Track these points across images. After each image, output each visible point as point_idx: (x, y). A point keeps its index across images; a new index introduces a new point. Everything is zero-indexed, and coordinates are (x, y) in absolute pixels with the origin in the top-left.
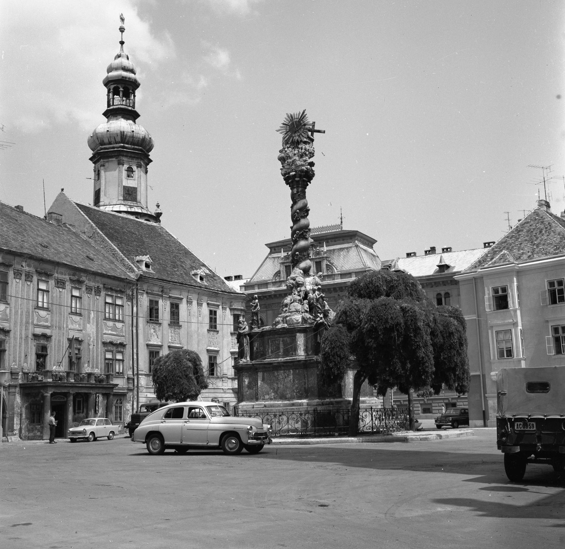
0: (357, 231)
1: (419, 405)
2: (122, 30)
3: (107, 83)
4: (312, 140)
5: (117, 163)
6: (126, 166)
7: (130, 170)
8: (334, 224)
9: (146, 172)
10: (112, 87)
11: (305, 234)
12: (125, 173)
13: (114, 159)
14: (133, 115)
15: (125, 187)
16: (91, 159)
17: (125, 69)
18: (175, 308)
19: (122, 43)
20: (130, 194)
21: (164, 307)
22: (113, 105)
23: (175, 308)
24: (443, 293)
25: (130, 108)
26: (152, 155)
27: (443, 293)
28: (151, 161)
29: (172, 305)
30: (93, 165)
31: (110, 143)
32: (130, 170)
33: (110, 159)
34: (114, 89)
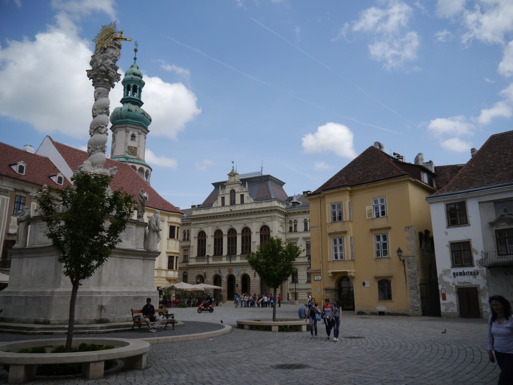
0: (269, 176)
1: (306, 293)
2: (136, 51)
4: (120, 47)
5: (125, 131)
6: (131, 133)
7: (133, 137)
9: (145, 138)
11: (100, 128)
12: (130, 138)
13: (123, 129)
15: (129, 147)
17: (134, 74)
19: (135, 59)
20: (133, 151)
28: (149, 131)
31: (122, 118)
32: (133, 137)
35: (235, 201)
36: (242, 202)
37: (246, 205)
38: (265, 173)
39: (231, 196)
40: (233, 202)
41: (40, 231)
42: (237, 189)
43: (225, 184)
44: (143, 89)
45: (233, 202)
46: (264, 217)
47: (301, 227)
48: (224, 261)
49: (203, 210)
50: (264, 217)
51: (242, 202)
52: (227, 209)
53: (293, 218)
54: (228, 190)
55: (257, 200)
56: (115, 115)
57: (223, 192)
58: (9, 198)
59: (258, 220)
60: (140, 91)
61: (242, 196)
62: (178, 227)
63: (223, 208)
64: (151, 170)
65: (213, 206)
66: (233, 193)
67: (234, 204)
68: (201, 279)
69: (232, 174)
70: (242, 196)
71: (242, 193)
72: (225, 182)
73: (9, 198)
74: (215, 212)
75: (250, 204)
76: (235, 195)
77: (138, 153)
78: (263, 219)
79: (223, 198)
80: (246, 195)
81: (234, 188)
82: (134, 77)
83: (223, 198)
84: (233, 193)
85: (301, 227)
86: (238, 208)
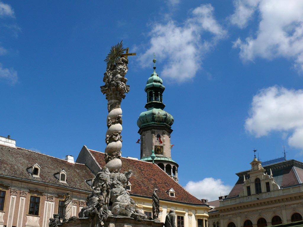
0: (293, 160)
3: (147, 89)
8: (280, 157)
10: (149, 91)
11: (114, 137)
13: (149, 131)
16: (139, 132)
26: (172, 127)
30: (140, 136)
33: (148, 131)
35: (260, 189)
36: (268, 190)
37: (272, 193)
38: (288, 158)
40: (258, 190)
43: (248, 173)
44: (163, 94)
45: (258, 190)
46: (294, 204)
49: (229, 201)
50: (294, 204)
51: (268, 190)
52: (253, 199)
58: (54, 203)
60: (161, 95)
62: (206, 221)
63: (249, 197)
64: (178, 166)
66: (258, 182)
67: (261, 192)
69: (255, 164)
70: (268, 184)
71: (267, 181)
72: (249, 171)
73: (54, 203)
76: (260, 184)
77: (164, 151)
78: (293, 206)
79: (249, 188)
81: (258, 177)
83: (249, 188)
84: (258, 182)
86: (265, 196)
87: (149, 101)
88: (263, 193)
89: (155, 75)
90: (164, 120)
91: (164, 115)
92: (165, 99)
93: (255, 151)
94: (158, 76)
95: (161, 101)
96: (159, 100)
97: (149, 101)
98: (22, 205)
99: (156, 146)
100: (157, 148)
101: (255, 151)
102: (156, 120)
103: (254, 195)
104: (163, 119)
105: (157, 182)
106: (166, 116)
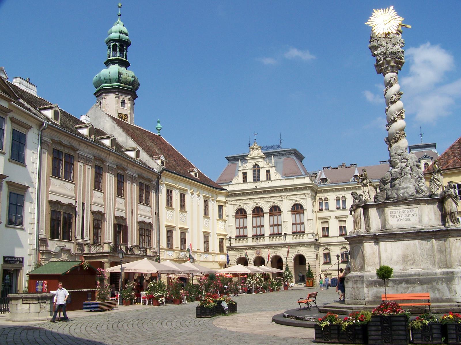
10: (112, 44)
14: (125, 64)
16: (95, 94)
17: (121, 32)
18: (182, 197)
21: (176, 195)
22: (112, 56)
23: (182, 197)
24: (340, 197)
25: (124, 59)
26: (138, 92)
27: (340, 197)
29: (181, 194)
31: (111, 82)
34: (113, 45)
35: (259, 177)
36: (268, 178)
39: (254, 171)
40: (257, 178)
41: (391, 217)
42: (262, 163)
45: (257, 178)
47: (333, 204)
48: (250, 242)
51: (268, 178)
52: (250, 186)
53: (323, 196)
54: (250, 165)
55: (286, 176)
56: (102, 78)
57: (244, 167)
59: (288, 198)
61: (268, 172)
63: (246, 184)
65: (233, 182)
66: (256, 169)
67: (259, 180)
68: (260, 261)
70: (268, 172)
71: (268, 169)
74: (235, 189)
75: (277, 180)
76: (259, 171)
79: (245, 174)
80: (273, 171)
81: (257, 163)
82: (122, 35)
83: (245, 174)
84: (256, 169)
85: (333, 204)
86: (263, 184)
87: (111, 56)
88: (262, 181)
89: (120, 24)
90: (131, 83)
91: (132, 77)
92: (131, 55)
93: (255, 135)
94: (123, 26)
95: (126, 58)
96: (125, 57)
97: (111, 56)
98: (88, 176)
99: (120, 114)
100: (121, 116)
101: (255, 135)
102: (121, 81)
103: (251, 182)
104: (130, 81)
105: (175, 159)
106: (134, 79)
